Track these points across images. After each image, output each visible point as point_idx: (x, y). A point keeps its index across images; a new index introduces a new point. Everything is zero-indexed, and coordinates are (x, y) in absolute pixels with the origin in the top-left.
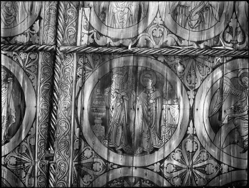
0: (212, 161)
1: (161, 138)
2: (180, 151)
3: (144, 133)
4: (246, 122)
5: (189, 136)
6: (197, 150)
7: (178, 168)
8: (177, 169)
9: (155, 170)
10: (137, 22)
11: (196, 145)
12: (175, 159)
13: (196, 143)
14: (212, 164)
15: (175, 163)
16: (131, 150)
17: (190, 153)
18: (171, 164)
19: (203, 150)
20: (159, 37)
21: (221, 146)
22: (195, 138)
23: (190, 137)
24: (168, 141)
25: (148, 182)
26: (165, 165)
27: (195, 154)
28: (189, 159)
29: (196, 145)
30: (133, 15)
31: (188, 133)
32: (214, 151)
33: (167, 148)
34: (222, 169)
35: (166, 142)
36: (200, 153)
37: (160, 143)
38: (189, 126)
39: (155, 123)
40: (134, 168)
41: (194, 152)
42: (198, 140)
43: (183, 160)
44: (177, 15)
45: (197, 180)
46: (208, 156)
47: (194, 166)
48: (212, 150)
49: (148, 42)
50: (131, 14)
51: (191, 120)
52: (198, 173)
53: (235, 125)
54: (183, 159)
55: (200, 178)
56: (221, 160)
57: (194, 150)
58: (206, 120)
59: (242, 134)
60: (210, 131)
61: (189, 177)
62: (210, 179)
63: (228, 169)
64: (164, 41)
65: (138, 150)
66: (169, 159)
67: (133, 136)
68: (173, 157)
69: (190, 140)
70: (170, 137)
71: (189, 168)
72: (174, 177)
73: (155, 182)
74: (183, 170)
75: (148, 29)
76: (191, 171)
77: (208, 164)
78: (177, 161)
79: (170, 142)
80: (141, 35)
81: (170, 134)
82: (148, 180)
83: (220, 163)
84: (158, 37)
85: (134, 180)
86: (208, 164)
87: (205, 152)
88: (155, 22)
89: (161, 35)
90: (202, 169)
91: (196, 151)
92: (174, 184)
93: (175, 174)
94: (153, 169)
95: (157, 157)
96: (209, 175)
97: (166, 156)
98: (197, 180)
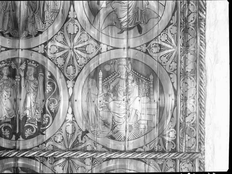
0: (92, 42)
1: (45, 23)
2: (62, 34)
3: (29, 18)
4: (123, 5)
5: (70, 20)
6: (77, 32)
7: (60, 50)
8: (60, 49)
9: (39, 52)
11: (77, 27)
12: (57, 41)
13: (77, 26)
14: (92, 45)
15: (58, 44)
16: (18, 34)
17: (72, 36)
18: (55, 46)
19: (83, 32)
21: (100, 28)
22: (76, 21)
23: (71, 20)
24: (51, 25)
27: (76, 35)
28: (71, 40)
29: (77, 27)
31: (69, 17)
32: (93, 33)
33: (50, 31)
34: (101, 49)
35: (49, 26)
36: (81, 35)
37: (43, 27)
38: (70, 10)
39: (39, 8)
40: (20, 50)
41: (75, 34)
42: (79, 23)
43: (65, 42)
45: (78, 59)
46: (89, 38)
47: (75, 47)
48: (92, 32)
51: (72, 5)
52: (79, 52)
53: (112, 8)
54: (65, 41)
55: (81, 57)
56: (100, 41)
57: (75, 32)
58: (86, 4)
59: (119, 17)
60: (89, 14)
62: (91, 58)
63: (107, 49)
65: (24, 34)
66: (53, 41)
67: (19, 22)
68: (56, 39)
69: (71, 24)
70: (53, 21)
71: (70, 49)
72: (57, 57)
73: (40, 62)
74: (65, 51)
76: (73, 52)
77: (88, 44)
78: (60, 42)
79: (53, 26)
81: (53, 19)
82: (33, 60)
83: (98, 43)
85: (20, 61)
86: (88, 44)
87: (85, 33)
90: (82, 49)
91: (76, 34)
92: (57, 64)
93: (58, 55)
94: (38, 51)
95: (42, 39)
96: (90, 55)
97: (49, 38)
98: (78, 59)
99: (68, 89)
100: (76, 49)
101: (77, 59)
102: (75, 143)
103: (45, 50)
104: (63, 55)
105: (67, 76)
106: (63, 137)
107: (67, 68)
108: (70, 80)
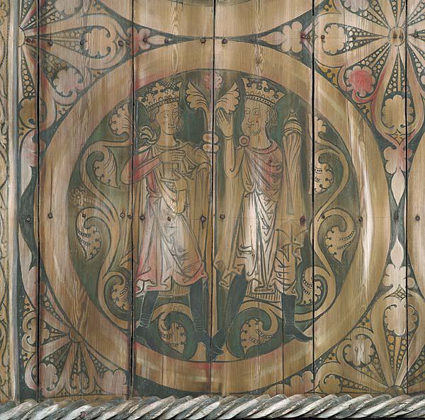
7: (360, 39)
9: (286, 48)
12: (349, 9)
15: (353, 21)
18: (339, 25)
25: (264, 84)
26: (319, 30)
28: (396, 6)
40: (218, 42)
43: (377, 12)
47: (411, 29)
54: (377, 8)
61: (396, 64)
71: (395, 37)
73: (288, 85)
74: (377, 44)
78: (357, 13)
82: (264, 79)
85: (218, 80)
93: (351, 57)
99: (389, 177)
100: (416, 35)
101: (420, 70)
102: (417, 367)
103: (306, 42)
104: (371, 59)
105: (383, 131)
106: (373, 346)
107: (384, 105)
108: (394, 148)
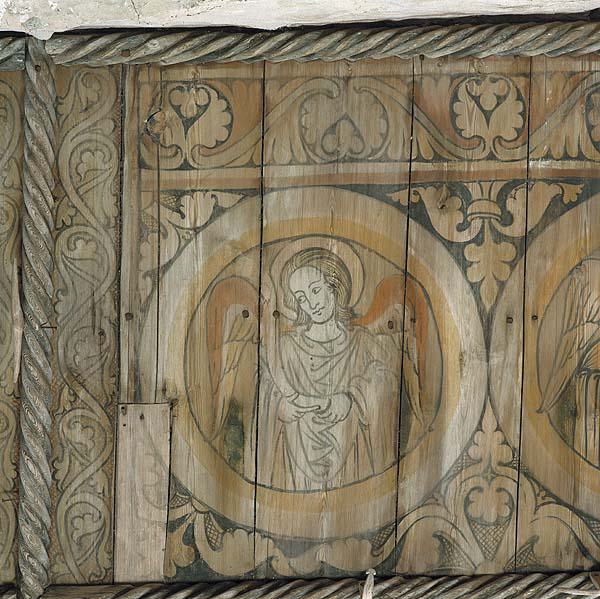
10: (391, 458)
20: (497, 523)
30: (374, 424)
44: (575, 414)
49: (445, 545)
50: (360, 423)
64: (521, 541)
75: (444, 486)
80: (413, 517)
84: (493, 519)
88: (473, 452)
89: (506, 512)
